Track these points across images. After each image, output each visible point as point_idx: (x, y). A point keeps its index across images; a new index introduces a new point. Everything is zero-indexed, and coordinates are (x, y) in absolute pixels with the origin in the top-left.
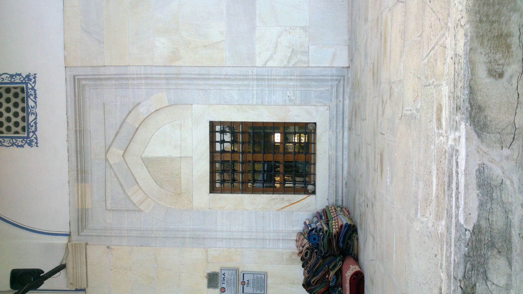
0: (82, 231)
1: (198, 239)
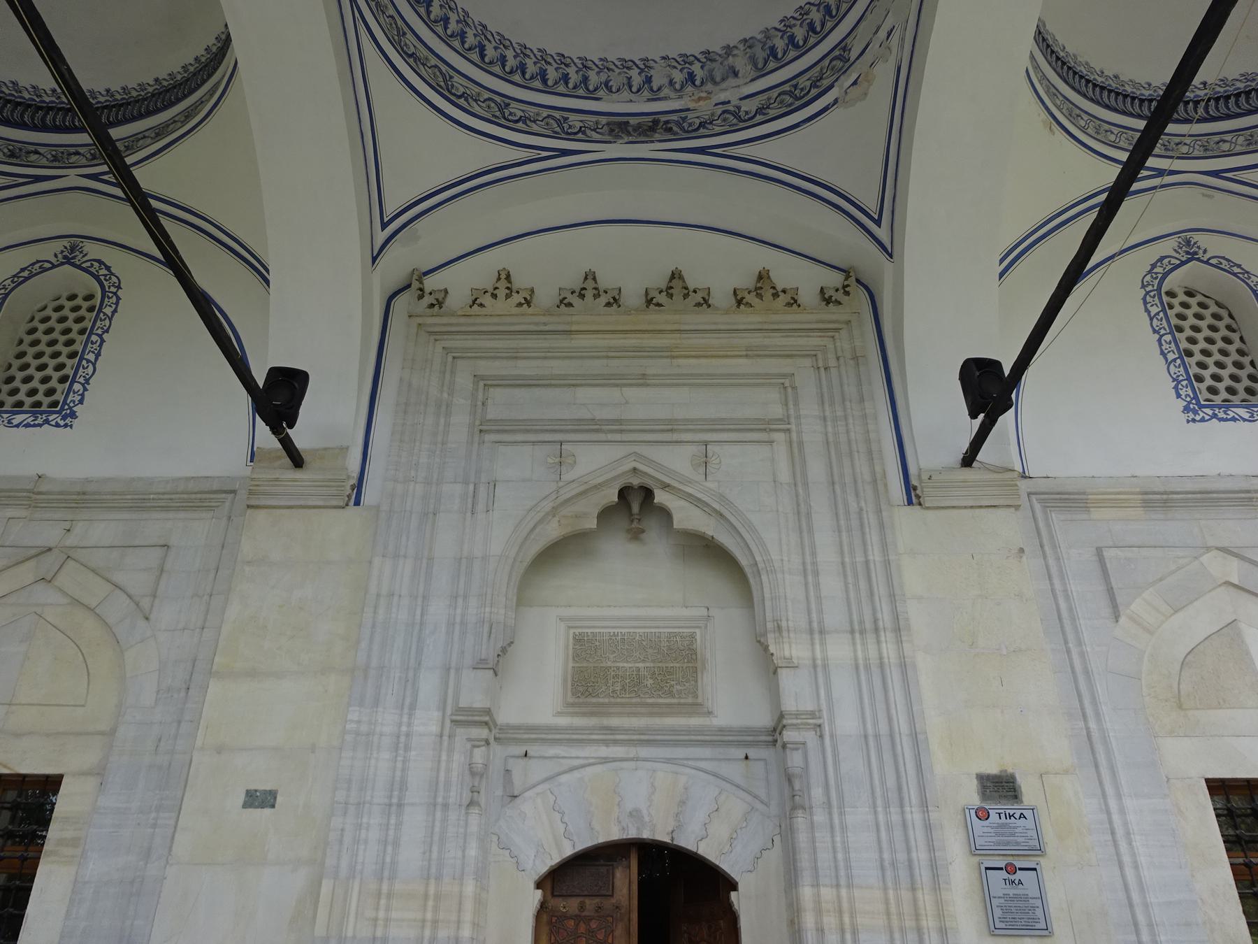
0: (1040, 501)
1: (1091, 747)
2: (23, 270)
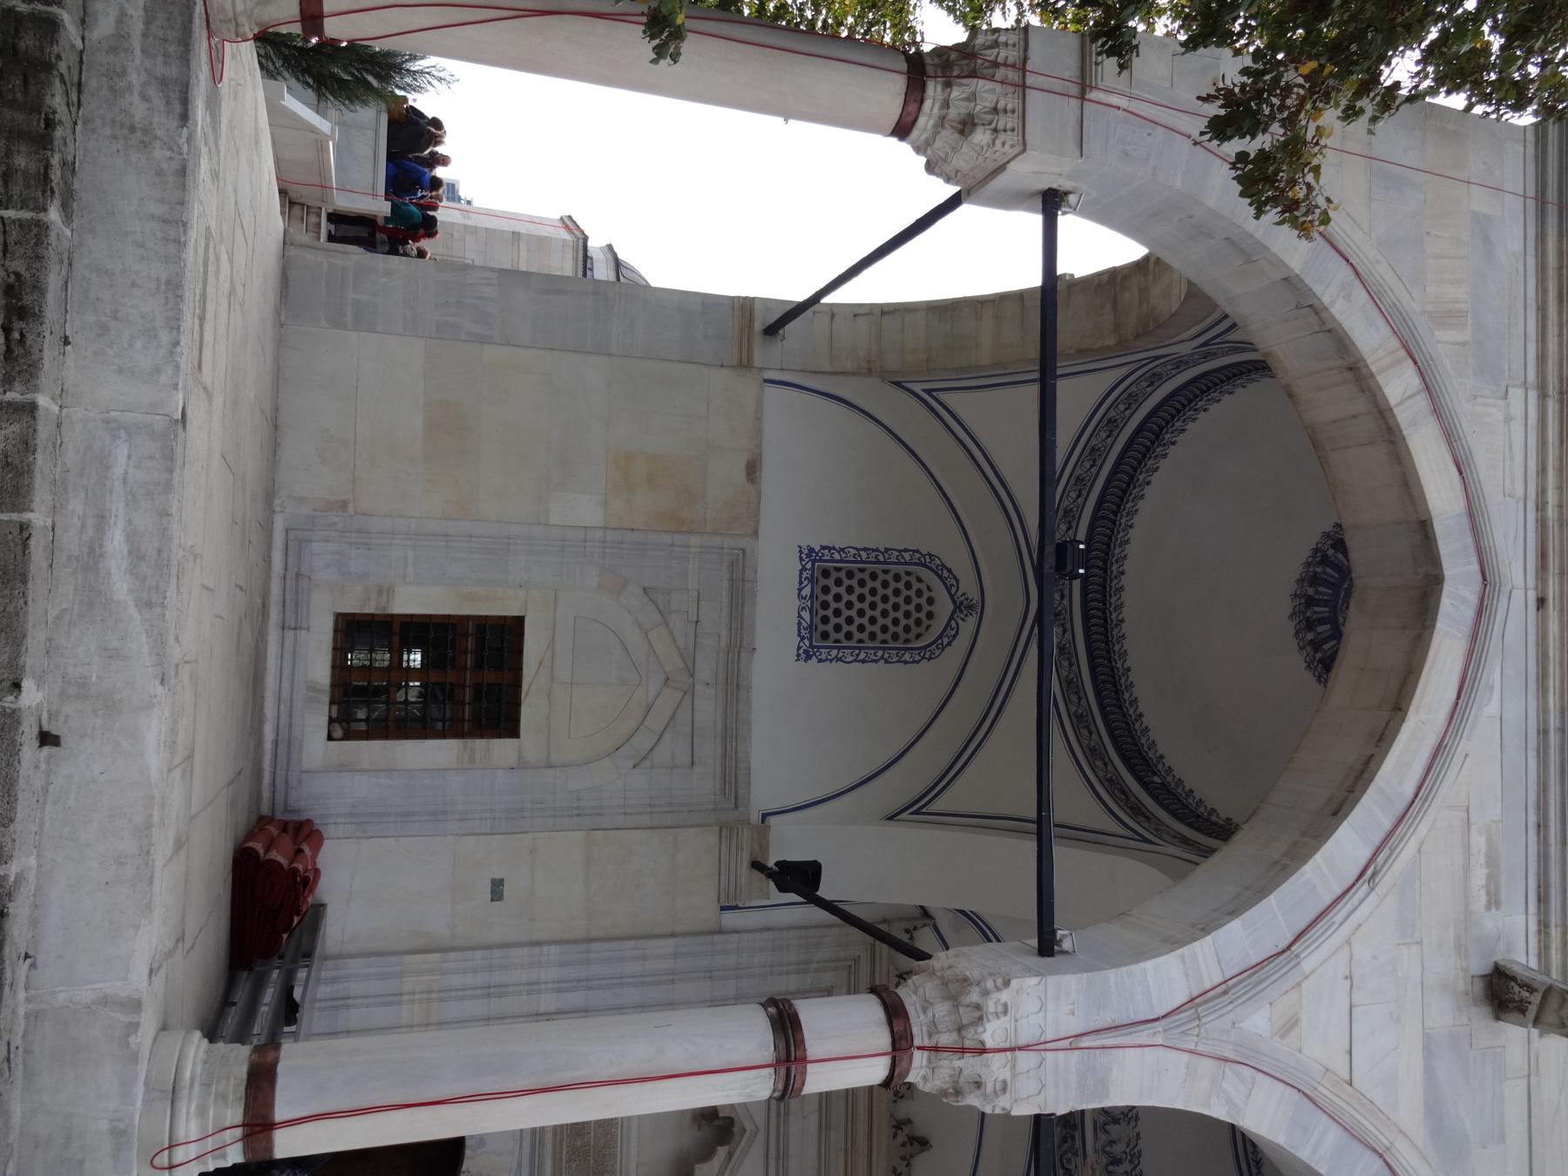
2: (949, 571)
